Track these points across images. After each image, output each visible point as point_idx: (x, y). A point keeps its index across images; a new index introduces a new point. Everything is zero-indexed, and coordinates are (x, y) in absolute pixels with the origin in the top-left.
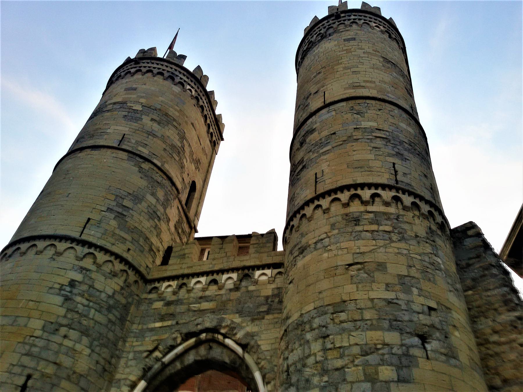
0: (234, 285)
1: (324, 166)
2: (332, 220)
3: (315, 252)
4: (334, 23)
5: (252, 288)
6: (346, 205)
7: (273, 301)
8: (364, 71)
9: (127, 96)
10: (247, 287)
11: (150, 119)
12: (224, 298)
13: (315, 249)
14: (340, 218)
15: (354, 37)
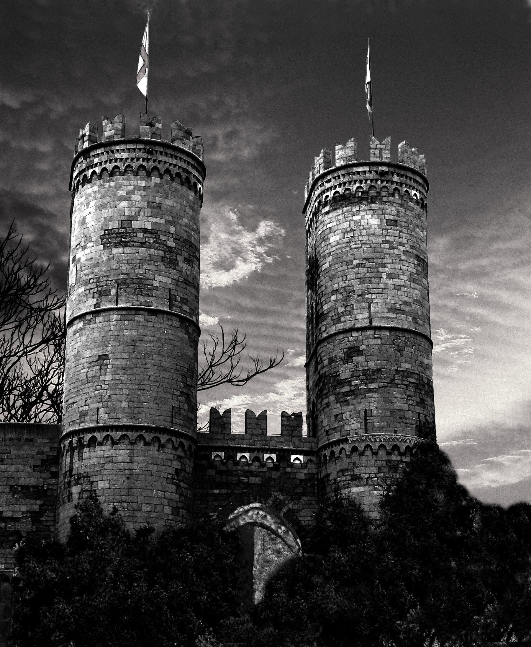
0: (274, 464)
1: (373, 405)
2: (379, 463)
3: (367, 487)
4: (377, 181)
5: (289, 470)
6: (389, 454)
7: (306, 485)
8: (403, 286)
9: (154, 220)
10: (284, 468)
11: (182, 258)
12: (268, 475)
13: (367, 484)
14: (384, 463)
15: (396, 218)
